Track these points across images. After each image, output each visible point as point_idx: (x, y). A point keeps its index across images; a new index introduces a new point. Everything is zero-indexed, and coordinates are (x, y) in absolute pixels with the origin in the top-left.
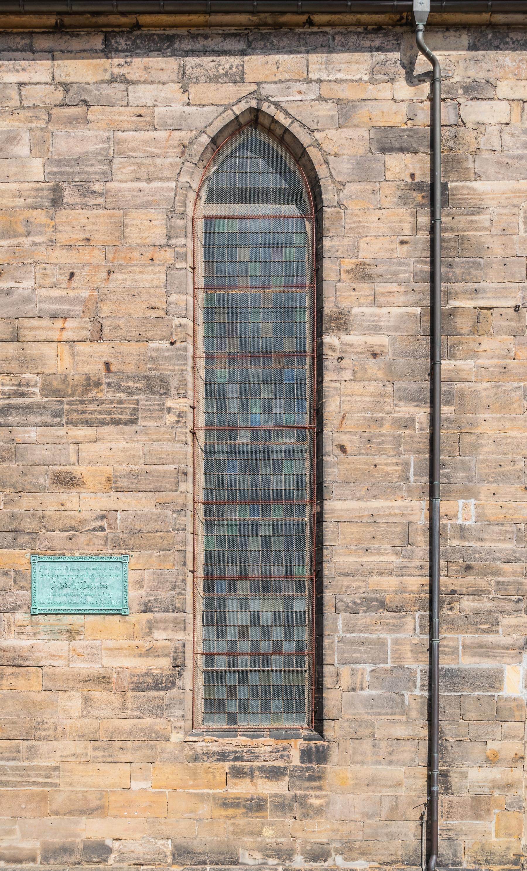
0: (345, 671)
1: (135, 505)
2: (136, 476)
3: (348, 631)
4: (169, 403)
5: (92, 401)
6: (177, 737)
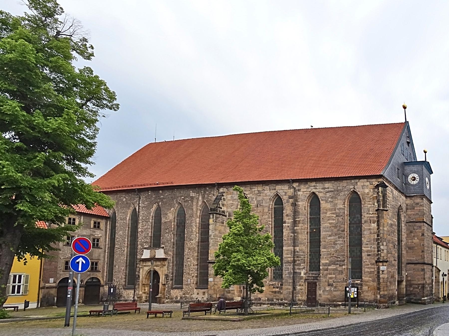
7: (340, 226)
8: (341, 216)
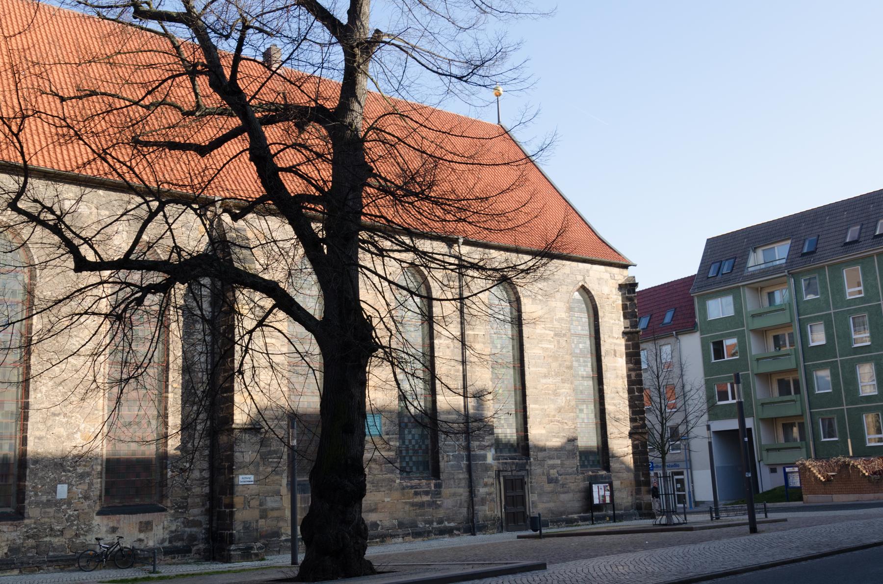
6: (398, 481)
8: (565, 335)
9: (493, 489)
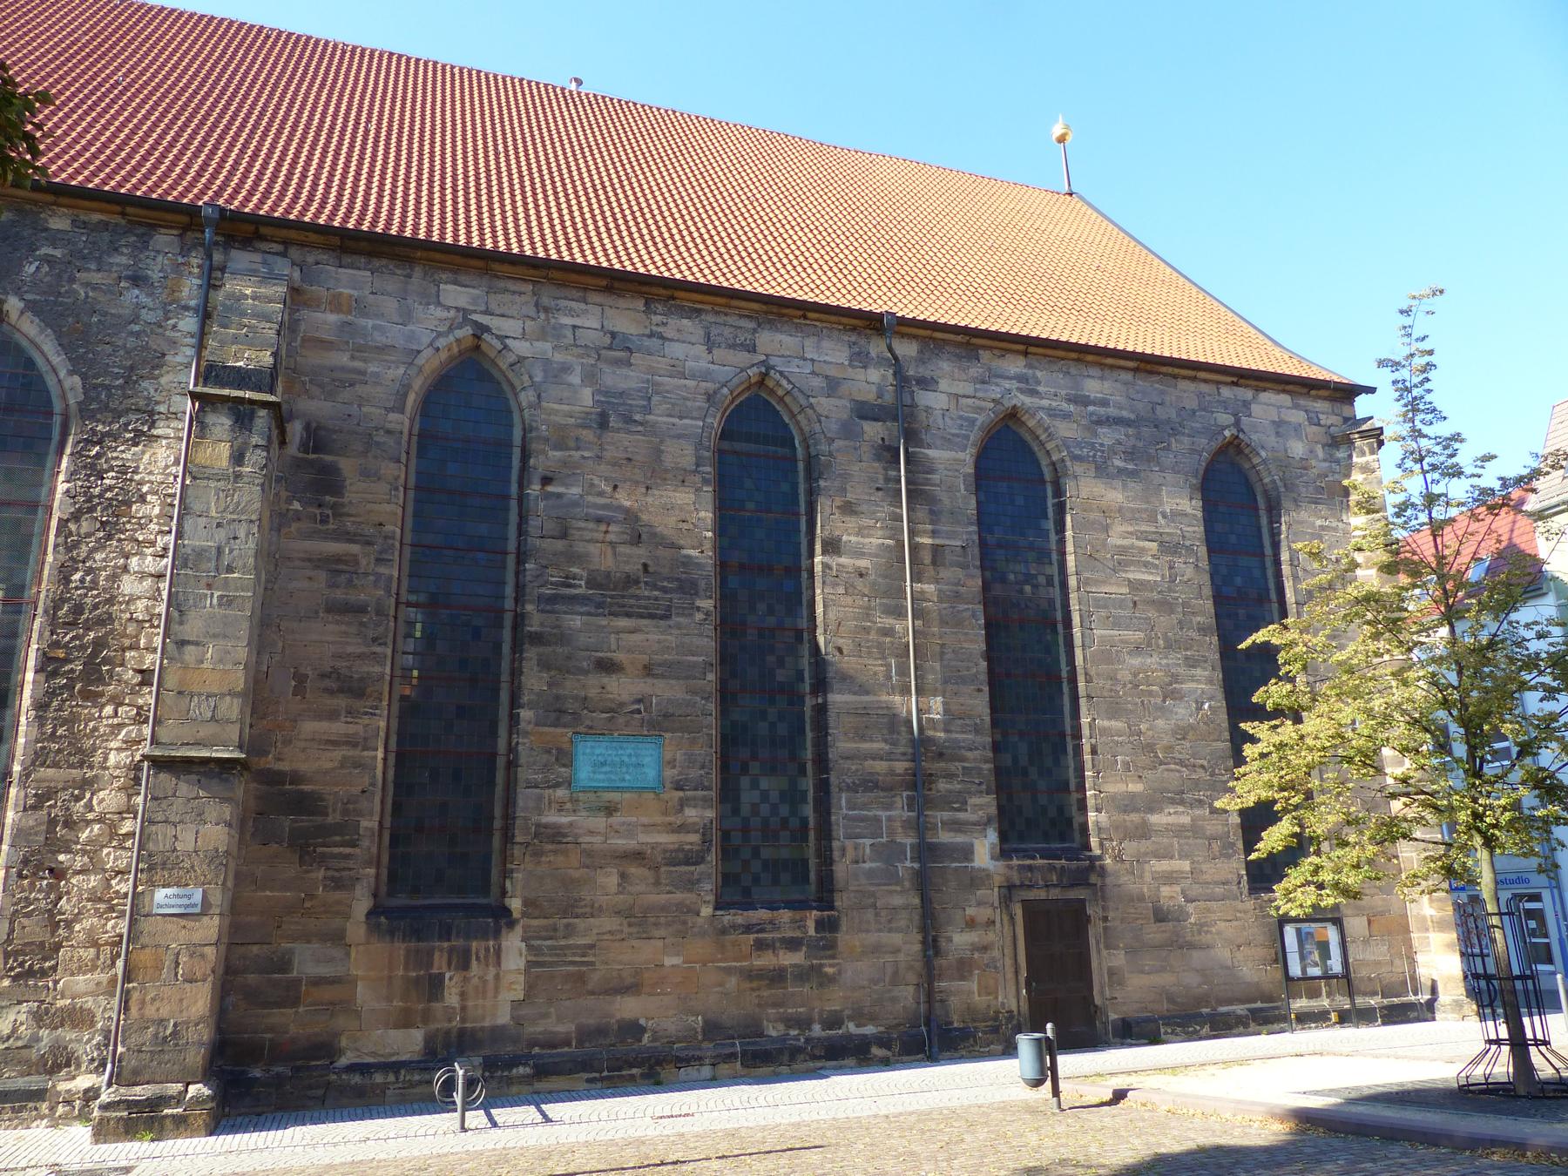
0: (849, 844)
1: (666, 691)
2: (669, 665)
3: (849, 809)
4: (699, 603)
5: (632, 596)
7: (1185, 605)
9: (991, 937)
